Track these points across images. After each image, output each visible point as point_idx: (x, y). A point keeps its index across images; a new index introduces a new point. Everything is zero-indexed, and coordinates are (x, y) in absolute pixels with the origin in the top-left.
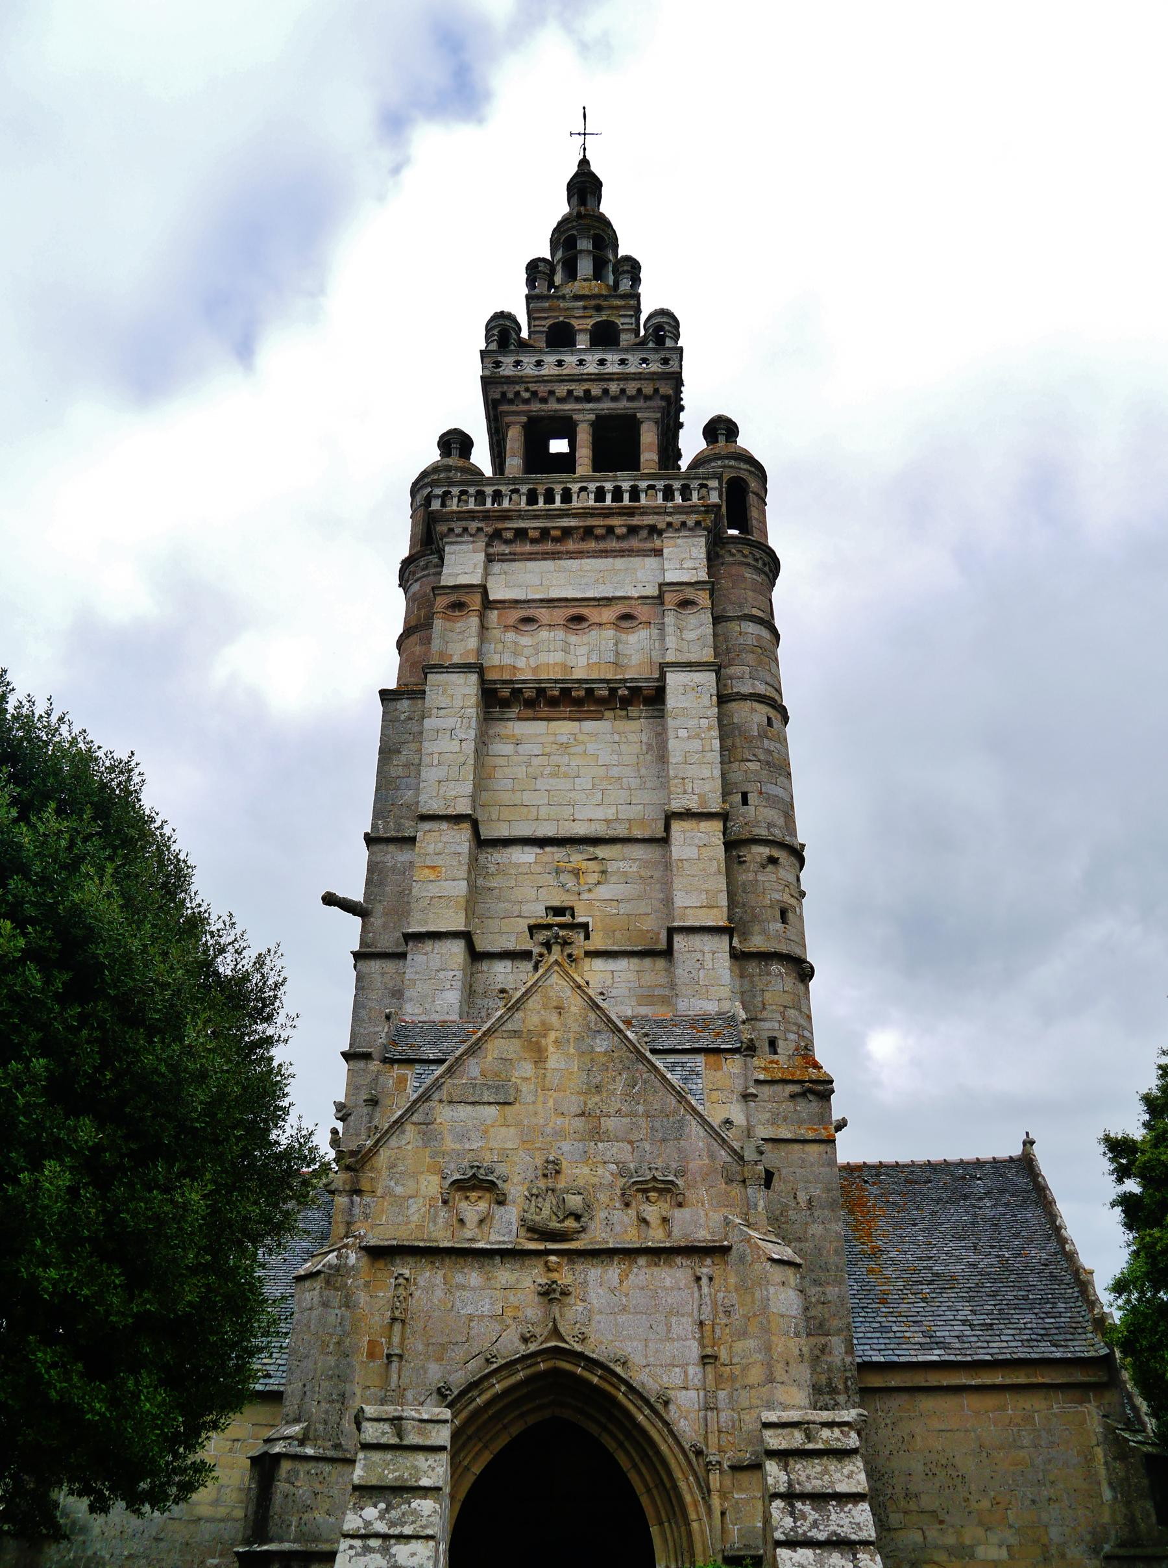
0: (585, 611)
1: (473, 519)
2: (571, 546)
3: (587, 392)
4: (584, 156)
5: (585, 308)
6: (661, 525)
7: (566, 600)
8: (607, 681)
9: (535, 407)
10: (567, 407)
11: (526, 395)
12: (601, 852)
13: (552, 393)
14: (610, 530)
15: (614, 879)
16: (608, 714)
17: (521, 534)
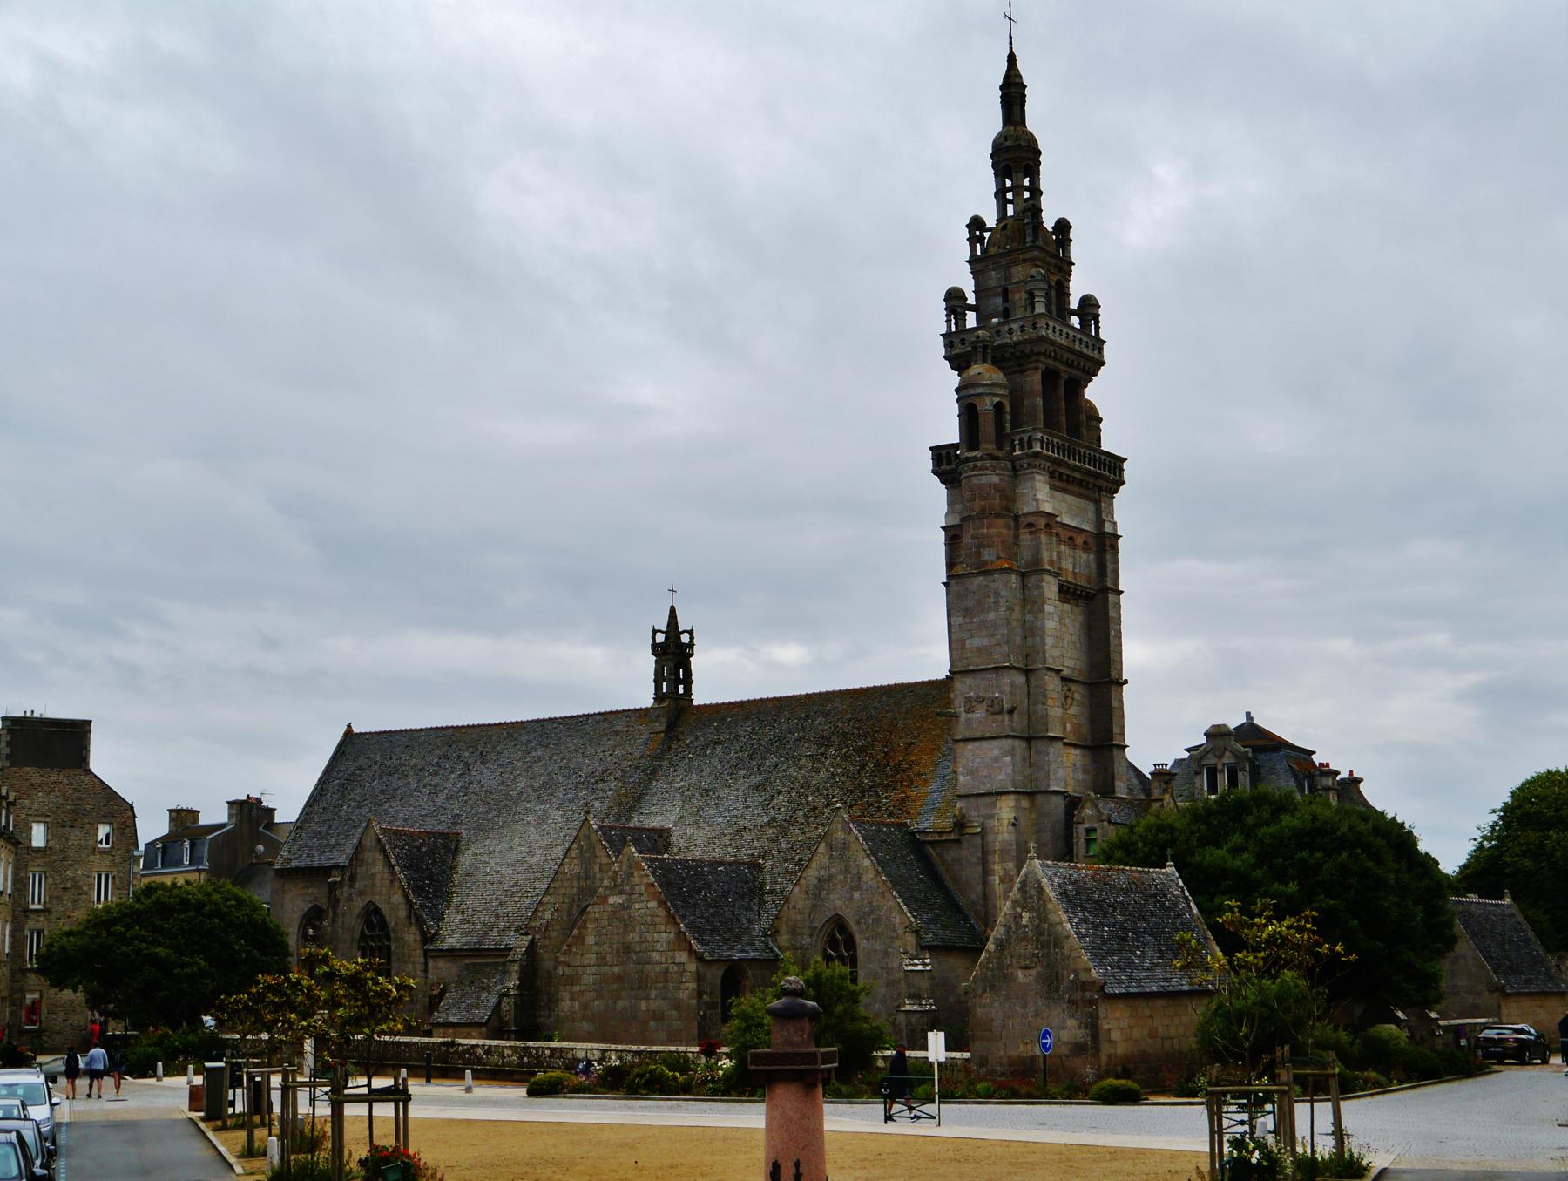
0: (1074, 535)
1: (1050, 461)
2: (1071, 487)
3: (1073, 361)
4: (1011, 48)
5: (1056, 266)
6: (1104, 488)
7: (1069, 526)
8: (1082, 587)
9: (1050, 362)
10: (1063, 367)
11: (1053, 354)
12: (1073, 687)
13: (1061, 356)
14: (1088, 483)
15: (1075, 703)
16: (1072, 602)
17: (1061, 474)
